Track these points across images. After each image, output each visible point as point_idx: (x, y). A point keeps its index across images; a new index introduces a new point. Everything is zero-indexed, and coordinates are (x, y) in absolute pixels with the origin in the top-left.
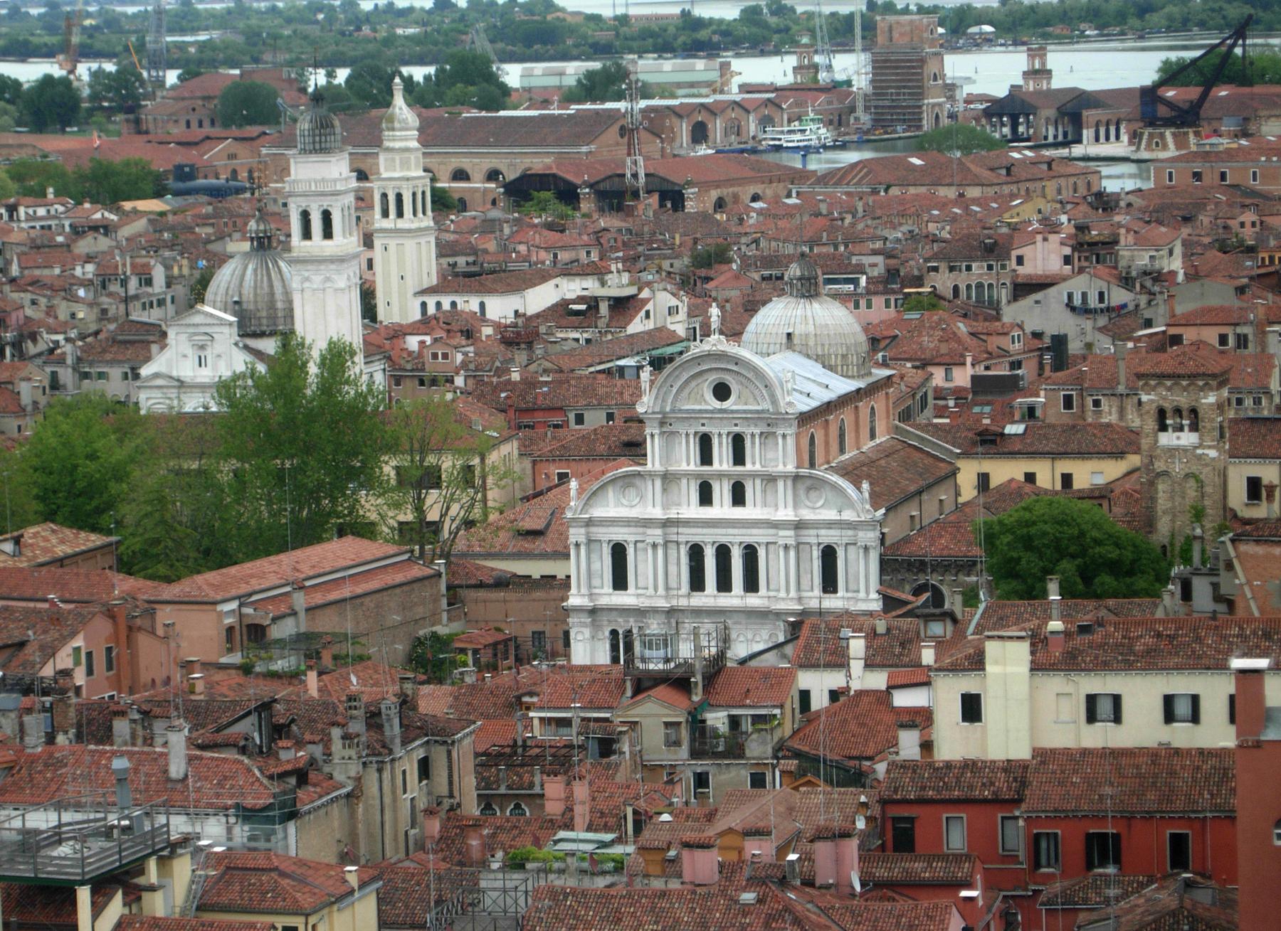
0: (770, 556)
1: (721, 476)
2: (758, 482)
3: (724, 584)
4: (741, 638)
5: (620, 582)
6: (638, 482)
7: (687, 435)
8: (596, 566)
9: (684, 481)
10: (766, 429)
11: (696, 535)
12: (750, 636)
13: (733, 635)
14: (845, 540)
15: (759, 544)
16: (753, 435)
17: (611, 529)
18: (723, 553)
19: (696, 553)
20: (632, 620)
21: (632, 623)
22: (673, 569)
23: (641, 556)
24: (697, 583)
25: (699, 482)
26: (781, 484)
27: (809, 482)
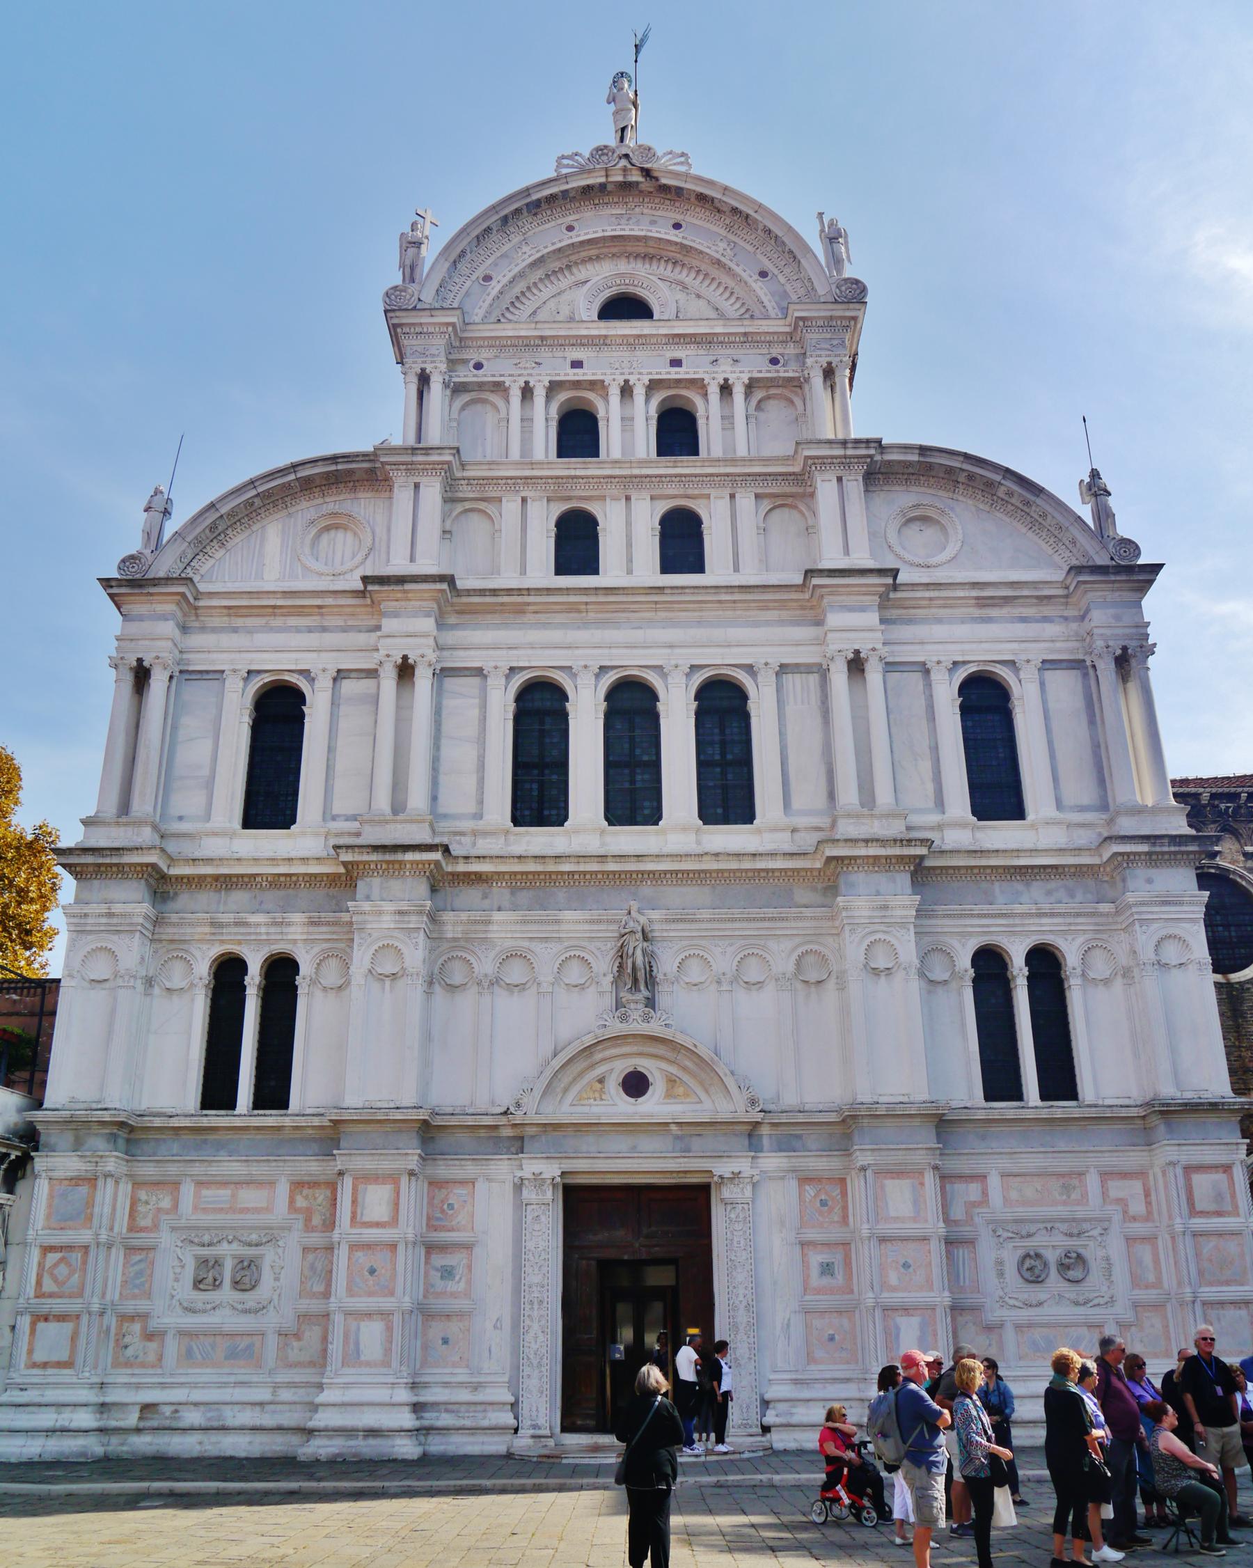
0: (789, 709)
1: (629, 484)
2: (746, 501)
3: (632, 798)
4: (695, 972)
5: (270, 799)
6: (363, 505)
7: (527, 392)
8: (193, 753)
9: (511, 506)
10: (767, 372)
11: (541, 648)
12: (723, 960)
13: (667, 964)
14: (1039, 652)
15: (750, 669)
16: (726, 389)
17: (263, 639)
18: (632, 705)
19: (540, 709)
20: (298, 917)
21: (297, 936)
22: (459, 755)
23: (352, 719)
24: (538, 797)
25: (558, 509)
26: (826, 488)
27: (904, 498)
